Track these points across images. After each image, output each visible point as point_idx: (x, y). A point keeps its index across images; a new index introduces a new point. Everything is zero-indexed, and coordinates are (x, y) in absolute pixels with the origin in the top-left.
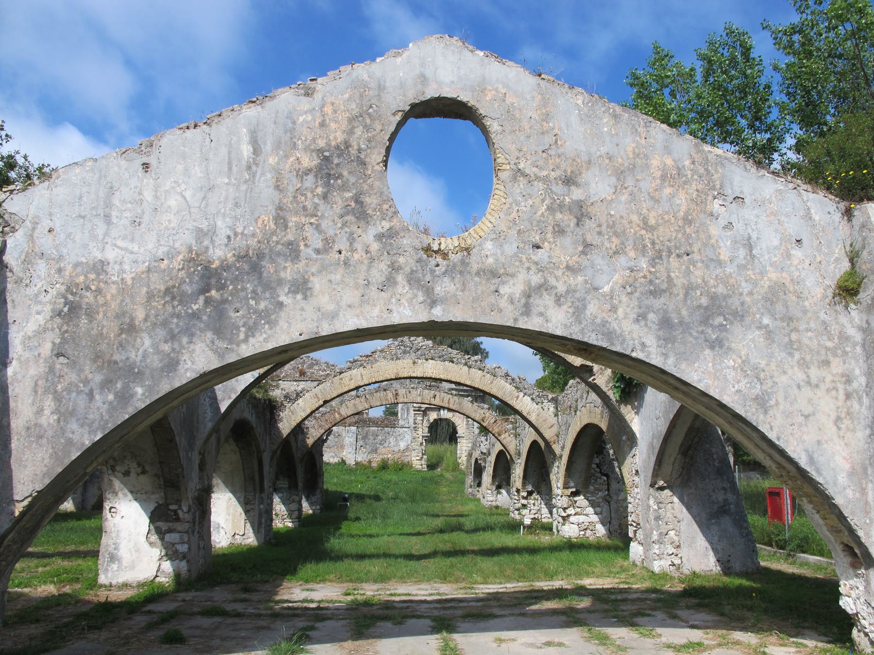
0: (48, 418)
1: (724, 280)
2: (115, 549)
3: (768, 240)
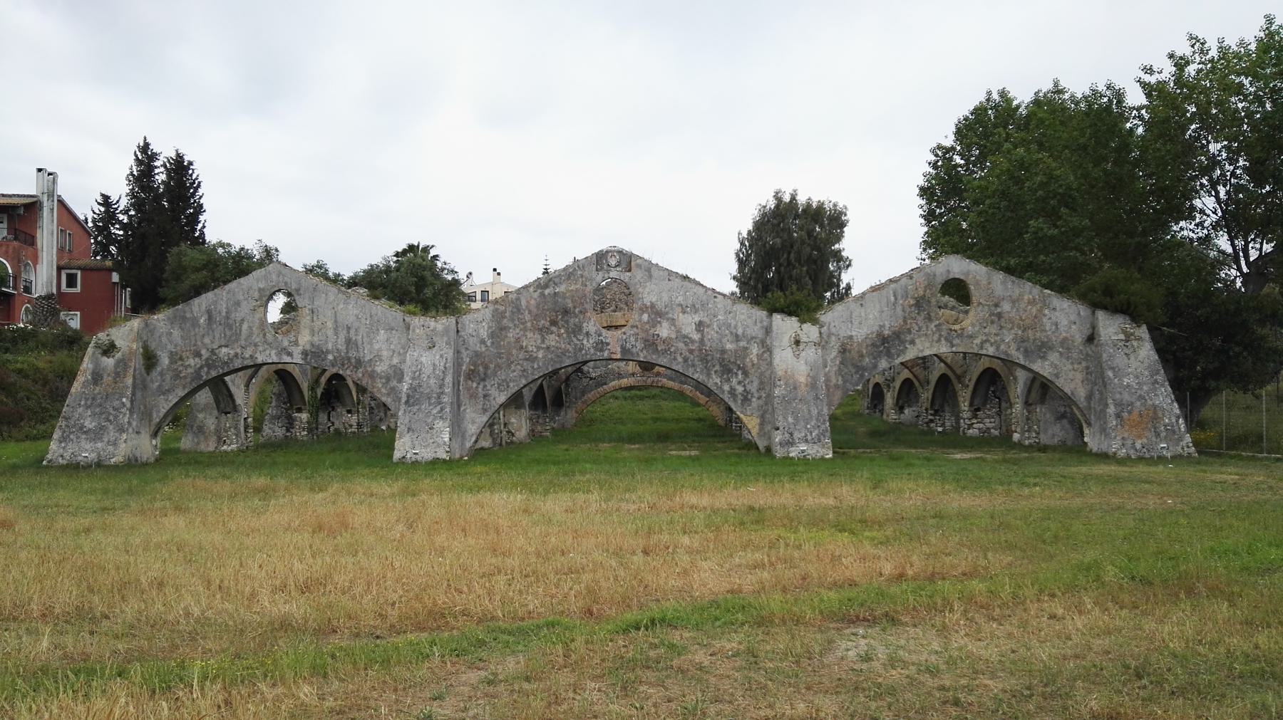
0: (840, 382)
1: (1047, 337)
3: (1064, 322)
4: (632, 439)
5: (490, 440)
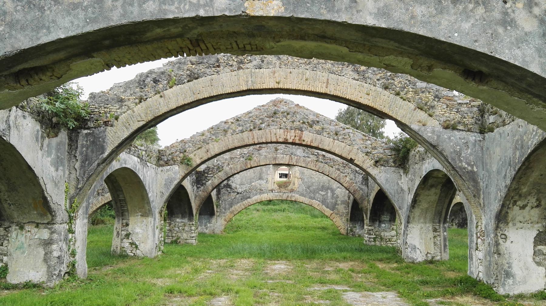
2: (509, 267)
4: (276, 252)
5: (44, 269)
